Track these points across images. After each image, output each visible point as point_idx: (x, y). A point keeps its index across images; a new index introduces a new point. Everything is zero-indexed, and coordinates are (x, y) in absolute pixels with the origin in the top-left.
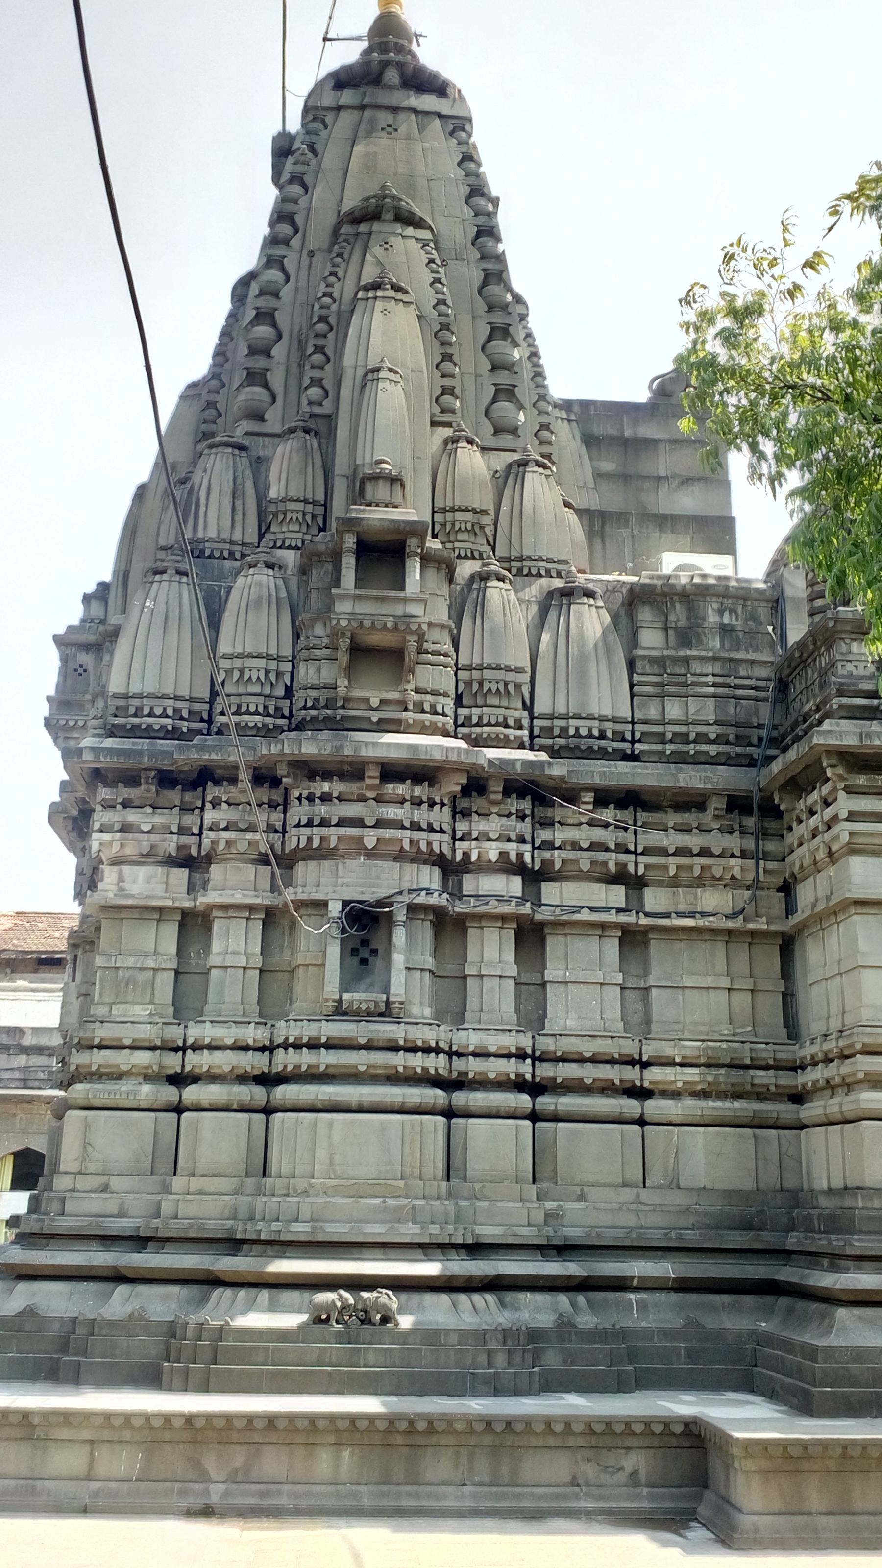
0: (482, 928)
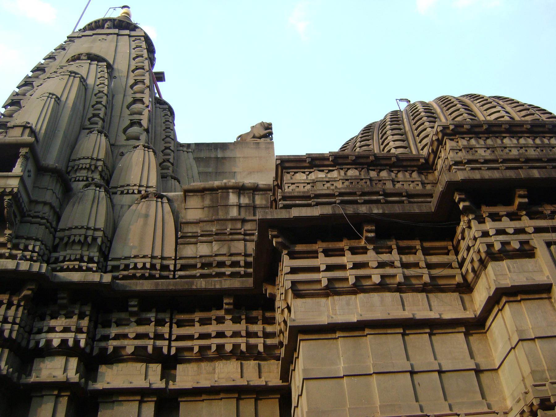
0: (42, 396)
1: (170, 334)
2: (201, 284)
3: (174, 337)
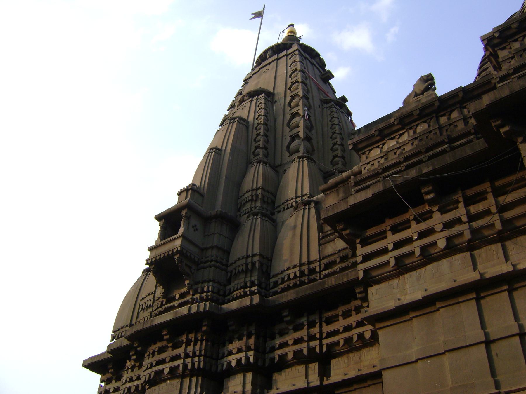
1: (321, 333)
2: (332, 281)
3: (324, 335)
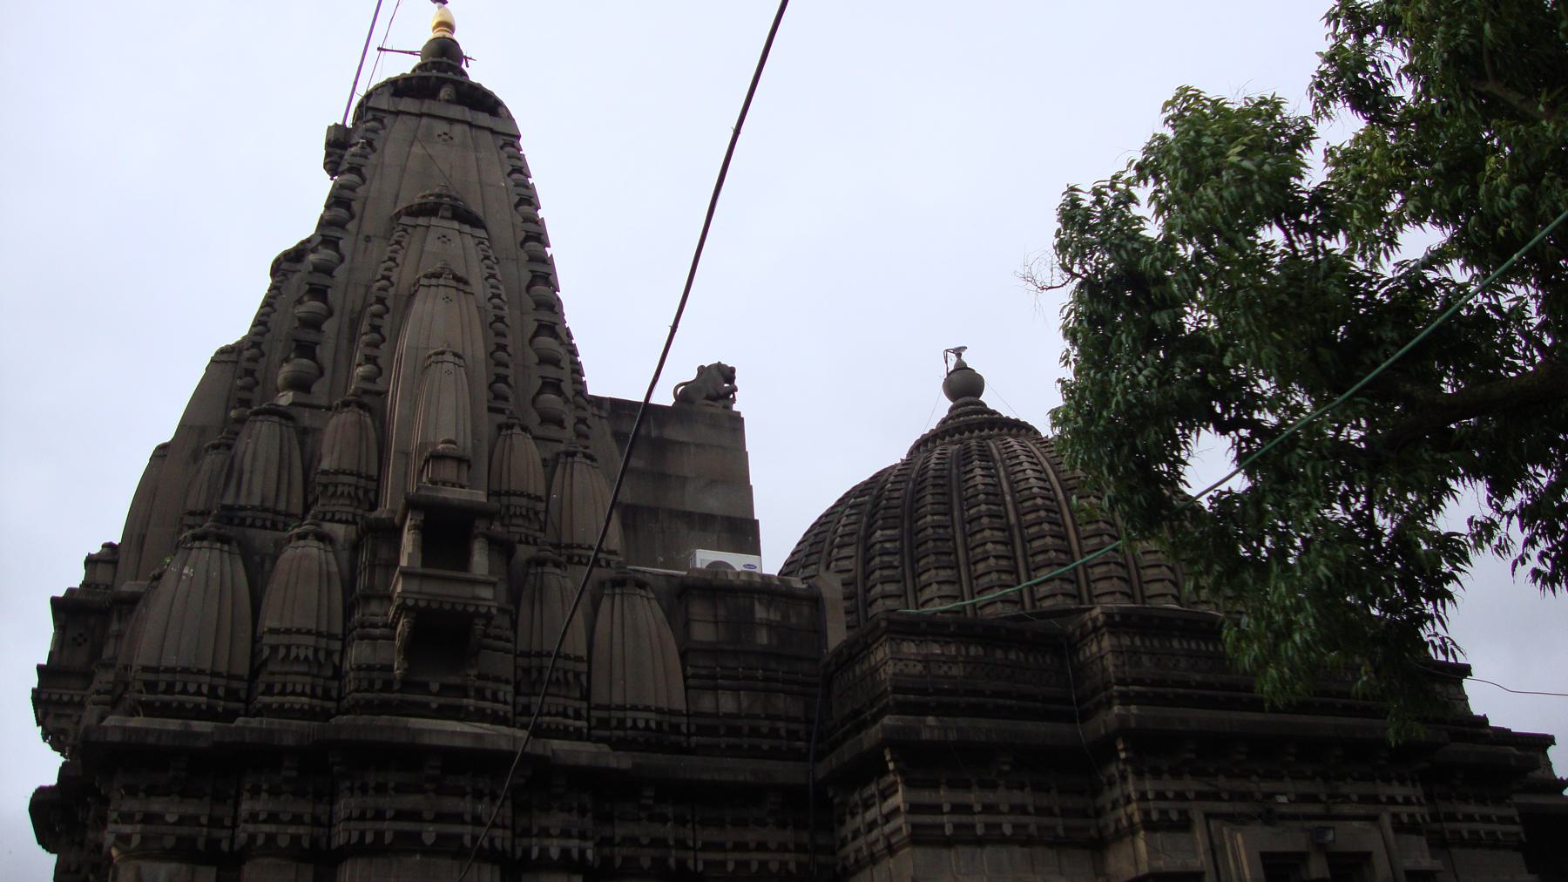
3: (699, 844)
